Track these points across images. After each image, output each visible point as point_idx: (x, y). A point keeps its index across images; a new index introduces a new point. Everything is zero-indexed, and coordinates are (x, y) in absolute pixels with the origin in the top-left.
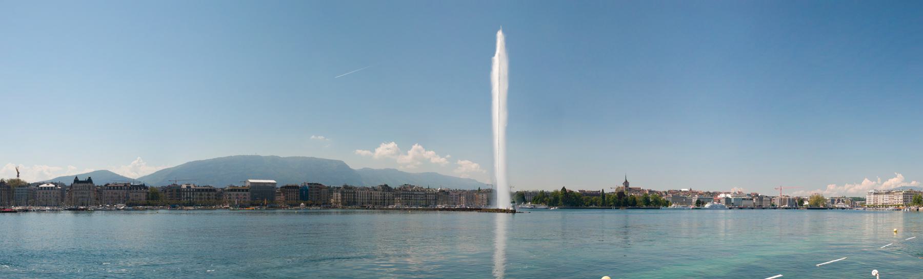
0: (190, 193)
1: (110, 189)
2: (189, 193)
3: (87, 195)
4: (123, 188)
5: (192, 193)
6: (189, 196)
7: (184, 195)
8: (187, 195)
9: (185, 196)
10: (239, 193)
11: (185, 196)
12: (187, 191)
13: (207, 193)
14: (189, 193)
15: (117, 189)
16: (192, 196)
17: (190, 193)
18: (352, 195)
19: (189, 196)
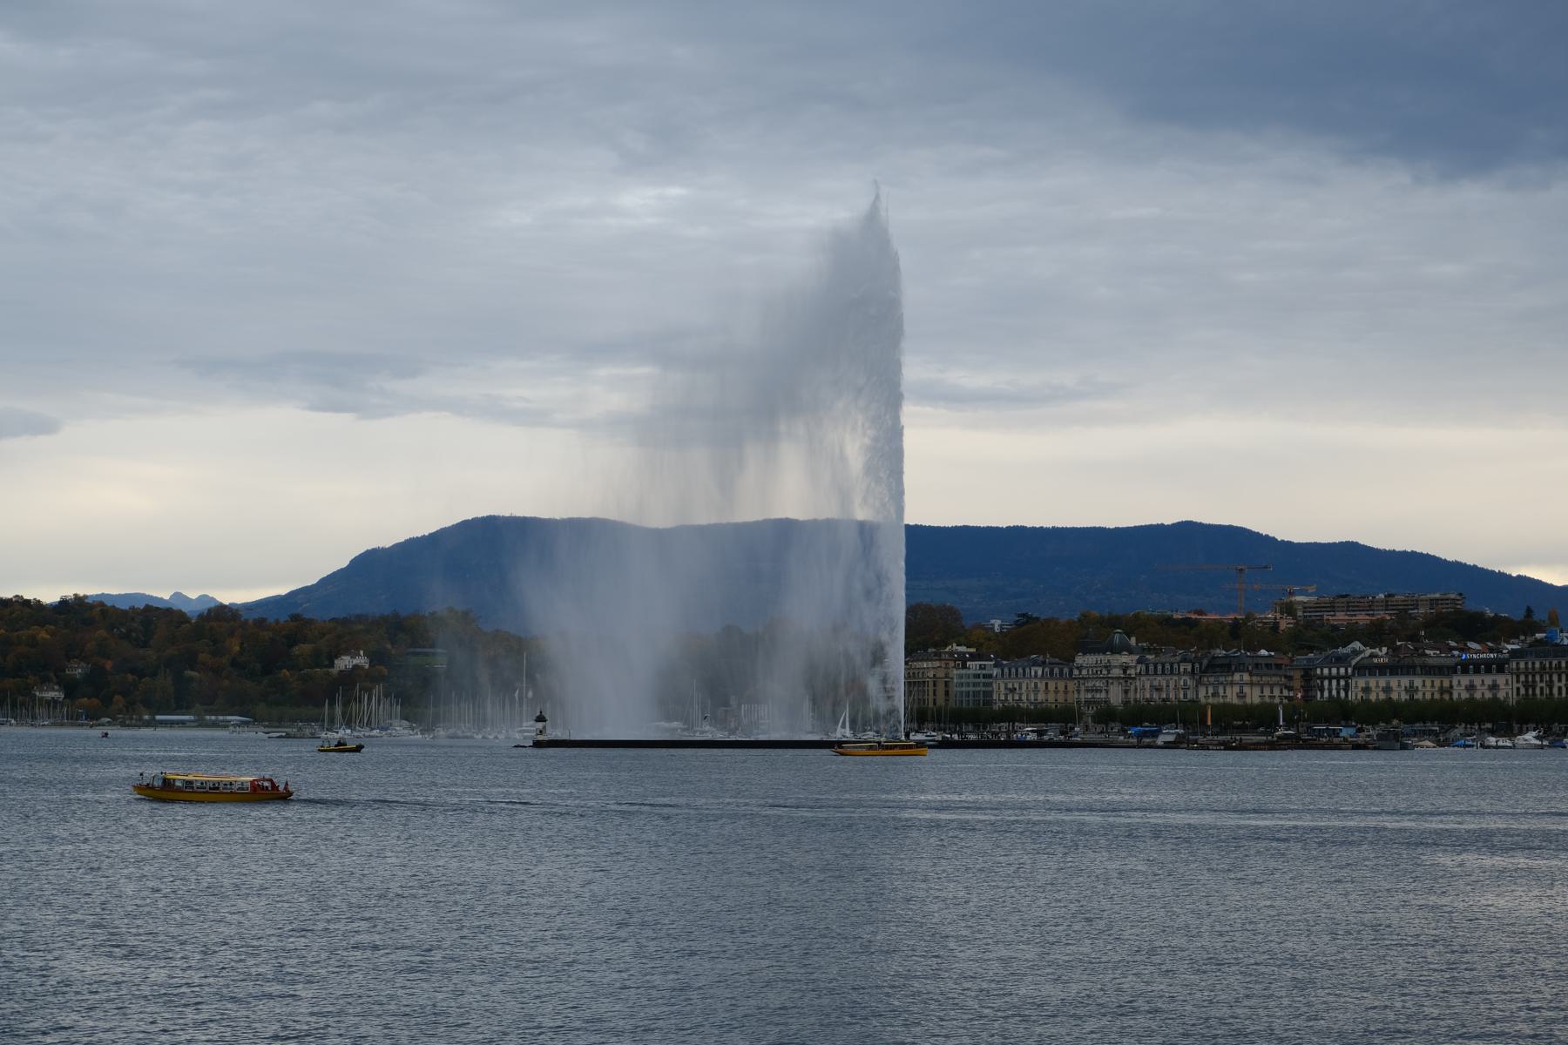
0: (1338, 684)
1: (1147, 673)
2: (1334, 682)
3: (1103, 695)
4: (1176, 666)
5: (1342, 683)
6: (1334, 693)
8: (1330, 692)
9: (1326, 694)
10: (1477, 680)
11: (1326, 694)
12: (1330, 678)
14: (1334, 682)
15: (1163, 673)
16: (1343, 694)
17: (1338, 684)
19: (1334, 693)
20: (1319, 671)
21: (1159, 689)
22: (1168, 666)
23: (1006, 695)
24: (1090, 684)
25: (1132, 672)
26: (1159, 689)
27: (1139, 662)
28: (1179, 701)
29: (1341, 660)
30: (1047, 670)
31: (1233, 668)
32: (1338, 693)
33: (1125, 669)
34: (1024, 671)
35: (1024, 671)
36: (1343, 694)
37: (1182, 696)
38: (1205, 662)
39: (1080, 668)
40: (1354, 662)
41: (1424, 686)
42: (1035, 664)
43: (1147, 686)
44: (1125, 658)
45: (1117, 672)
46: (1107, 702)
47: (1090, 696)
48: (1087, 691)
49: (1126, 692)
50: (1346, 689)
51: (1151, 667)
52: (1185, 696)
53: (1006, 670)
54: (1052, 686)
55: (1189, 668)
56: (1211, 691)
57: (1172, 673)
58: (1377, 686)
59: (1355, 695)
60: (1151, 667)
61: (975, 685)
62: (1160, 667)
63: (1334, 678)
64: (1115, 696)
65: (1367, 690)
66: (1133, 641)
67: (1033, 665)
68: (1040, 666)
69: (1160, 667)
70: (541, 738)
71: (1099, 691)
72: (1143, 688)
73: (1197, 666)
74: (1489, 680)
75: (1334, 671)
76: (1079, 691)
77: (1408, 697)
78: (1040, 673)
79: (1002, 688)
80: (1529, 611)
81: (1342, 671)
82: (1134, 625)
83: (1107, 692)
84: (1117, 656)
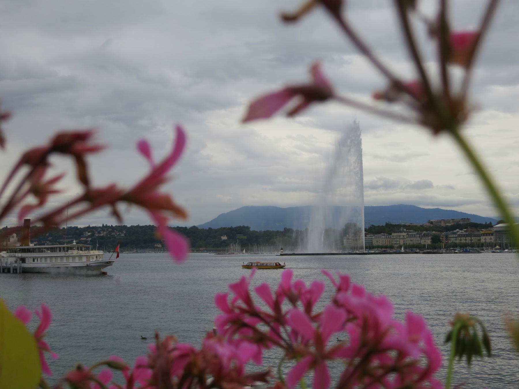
0: (454, 239)
1: (409, 237)
2: (453, 238)
3: (399, 242)
4: (416, 235)
5: (455, 238)
6: (453, 241)
8: (452, 241)
9: (451, 241)
10: (487, 237)
11: (451, 241)
12: (452, 238)
13: (464, 238)
14: (453, 238)
16: (455, 241)
17: (454, 239)
19: (453, 241)
20: (449, 236)
21: (412, 241)
22: (414, 235)
23: (376, 243)
24: (395, 240)
25: (405, 237)
26: (412, 241)
27: (407, 235)
28: (417, 243)
29: (454, 233)
30: (385, 237)
31: (429, 235)
32: (454, 241)
33: (404, 236)
34: (380, 237)
35: (380, 237)
36: (455, 241)
37: (417, 242)
38: (422, 234)
39: (393, 236)
40: (457, 234)
41: (474, 239)
42: (383, 235)
43: (409, 240)
44: (403, 234)
45: (402, 237)
46: (400, 244)
47: (395, 242)
48: (395, 241)
49: (404, 241)
50: (456, 240)
51: (410, 236)
52: (418, 242)
53: (376, 237)
54: (386, 240)
55: (419, 236)
56: (424, 241)
58: (463, 239)
59: (458, 241)
60: (410, 236)
61: (369, 240)
62: (412, 236)
63: (453, 237)
64: (402, 242)
65: (461, 240)
66: (405, 230)
67: (382, 236)
68: (383, 236)
69: (412, 236)
70: (282, 253)
71: (397, 241)
72: (408, 241)
73: (420, 235)
74: (489, 237)
75: (453, 236)
76: (393, 241)
77: (470, 241)
78: (384, 238)
79: (375, 240)
80: (486, 223)
81: (455, 236)
82: (405, 226)
83: (400, 242)
84: (402, 233)
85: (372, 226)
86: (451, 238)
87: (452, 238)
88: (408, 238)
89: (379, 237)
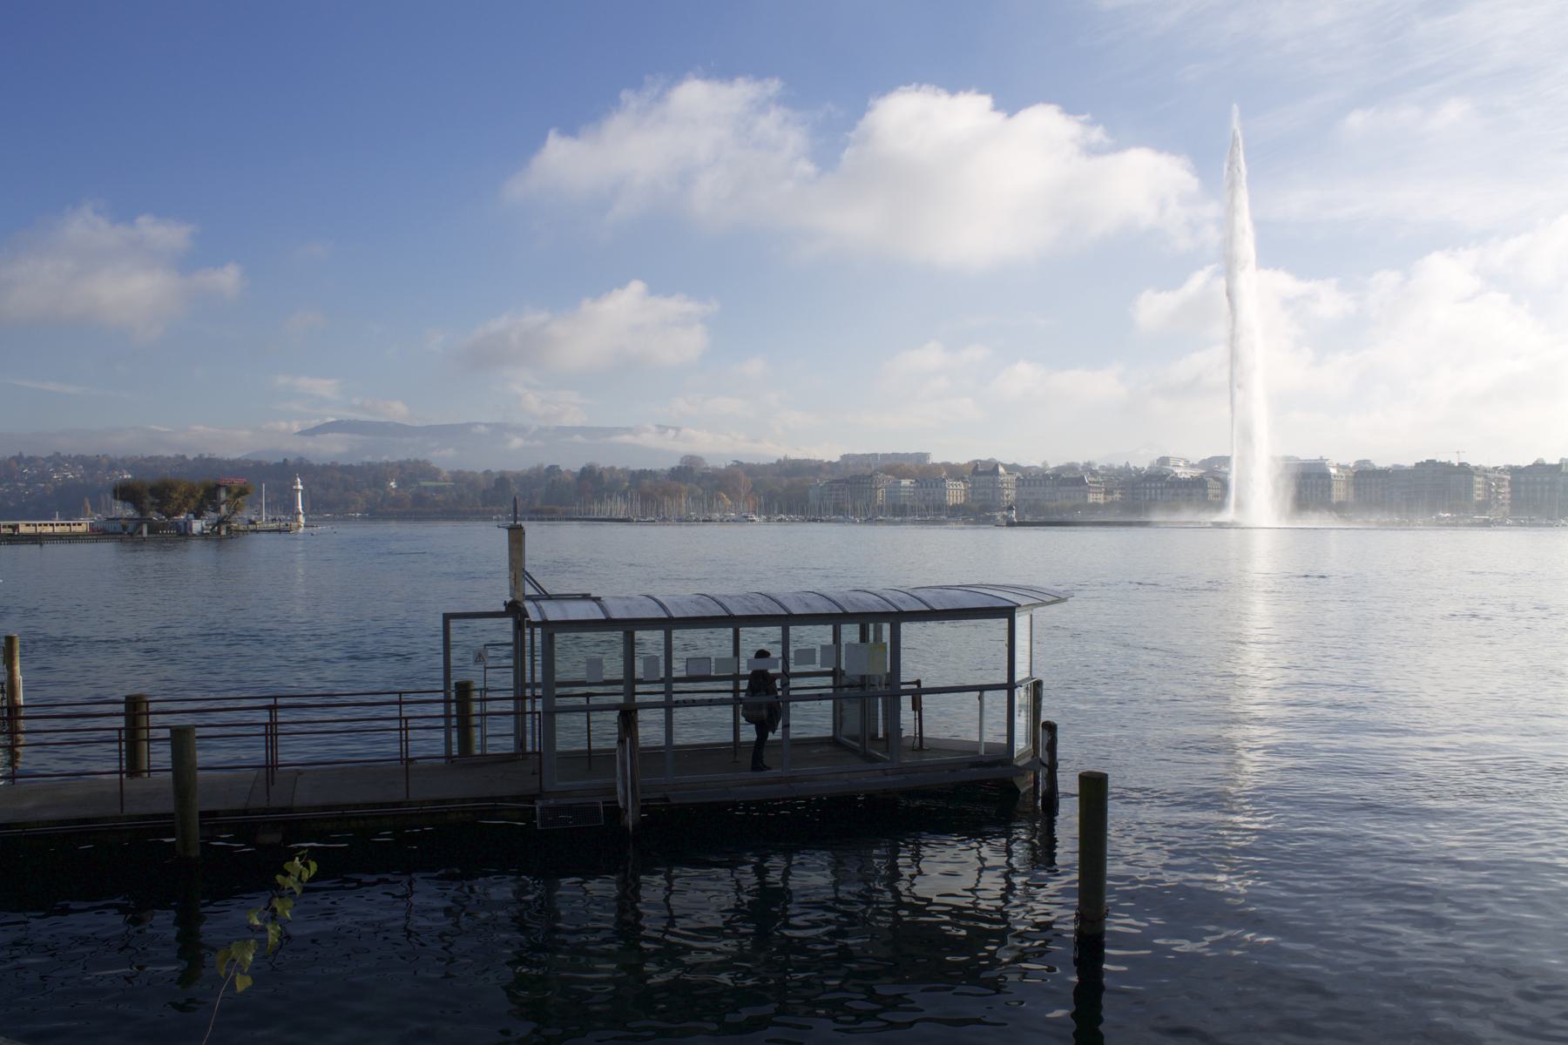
2: (1153, 491)
4: (1043, 482)
6: (1153, 496)
7: (1145, 495)
9: (1147, 497)
11: (1147, 497)
12: (1150, 488)
14: (1153, 491)
16: (1159, 497)
18: (1547, 487)
19: (1153, 496)
27: (1018, 479)
57: (1041, 485)
62: (1032, 483)
69: (1032, 483)
85: (735, 464)
86: (1148, 491)
87: (1150, 488)
88: (1021, 488)
89: (929, 485)
